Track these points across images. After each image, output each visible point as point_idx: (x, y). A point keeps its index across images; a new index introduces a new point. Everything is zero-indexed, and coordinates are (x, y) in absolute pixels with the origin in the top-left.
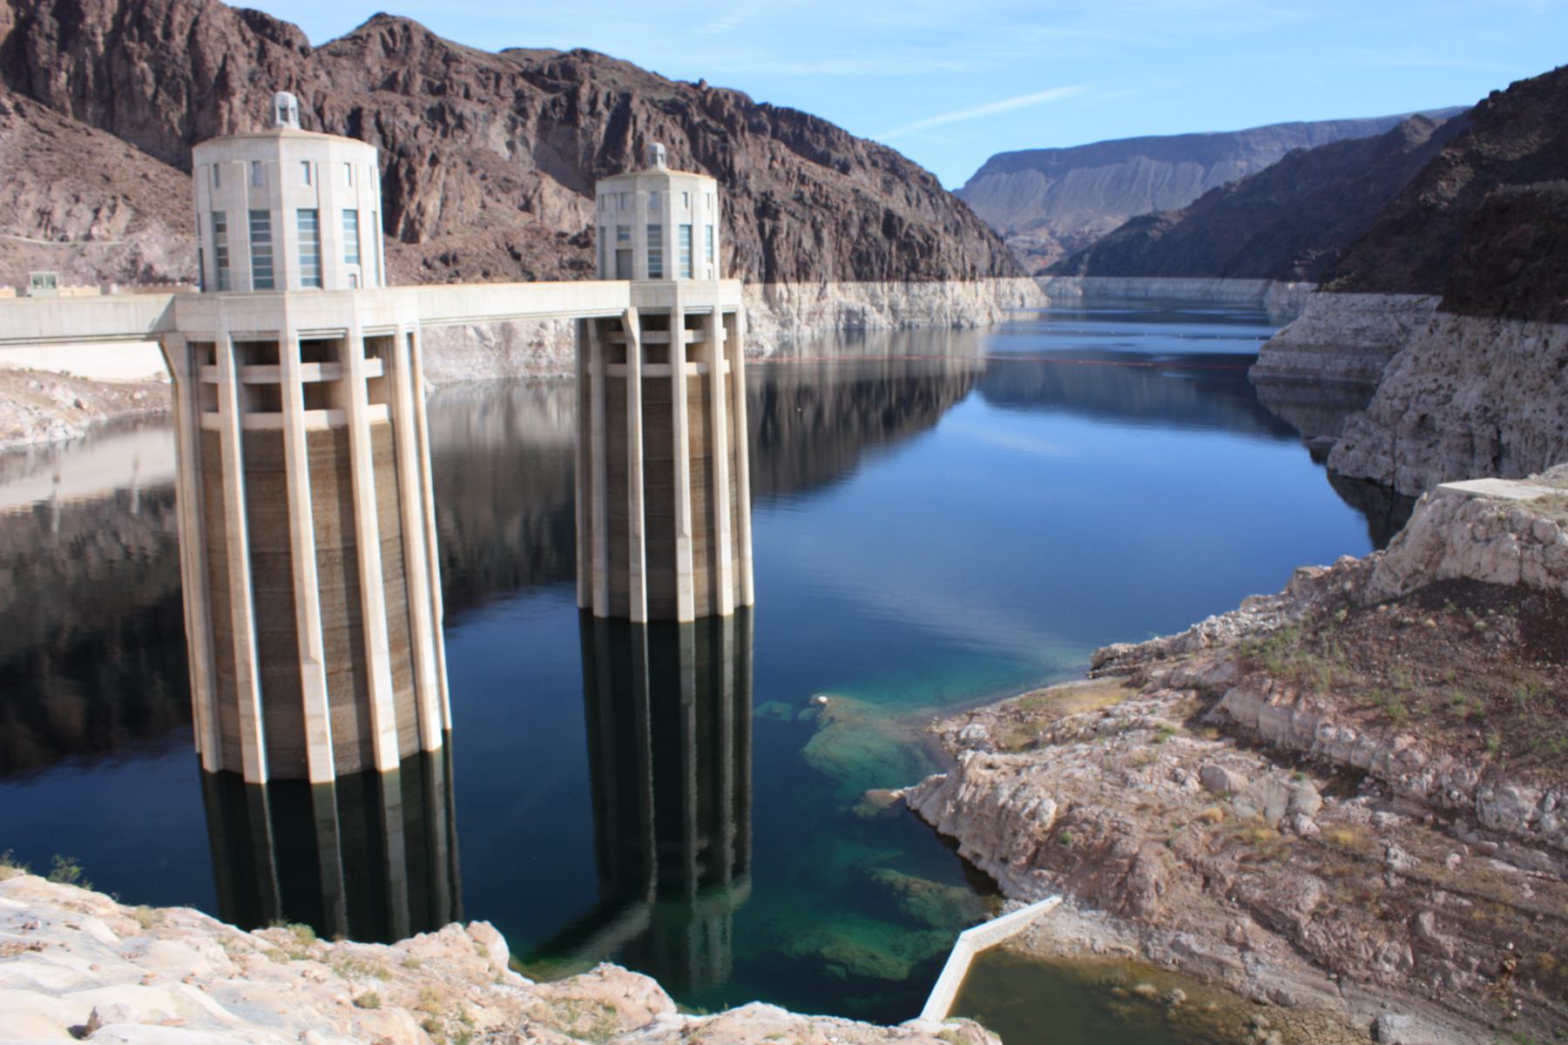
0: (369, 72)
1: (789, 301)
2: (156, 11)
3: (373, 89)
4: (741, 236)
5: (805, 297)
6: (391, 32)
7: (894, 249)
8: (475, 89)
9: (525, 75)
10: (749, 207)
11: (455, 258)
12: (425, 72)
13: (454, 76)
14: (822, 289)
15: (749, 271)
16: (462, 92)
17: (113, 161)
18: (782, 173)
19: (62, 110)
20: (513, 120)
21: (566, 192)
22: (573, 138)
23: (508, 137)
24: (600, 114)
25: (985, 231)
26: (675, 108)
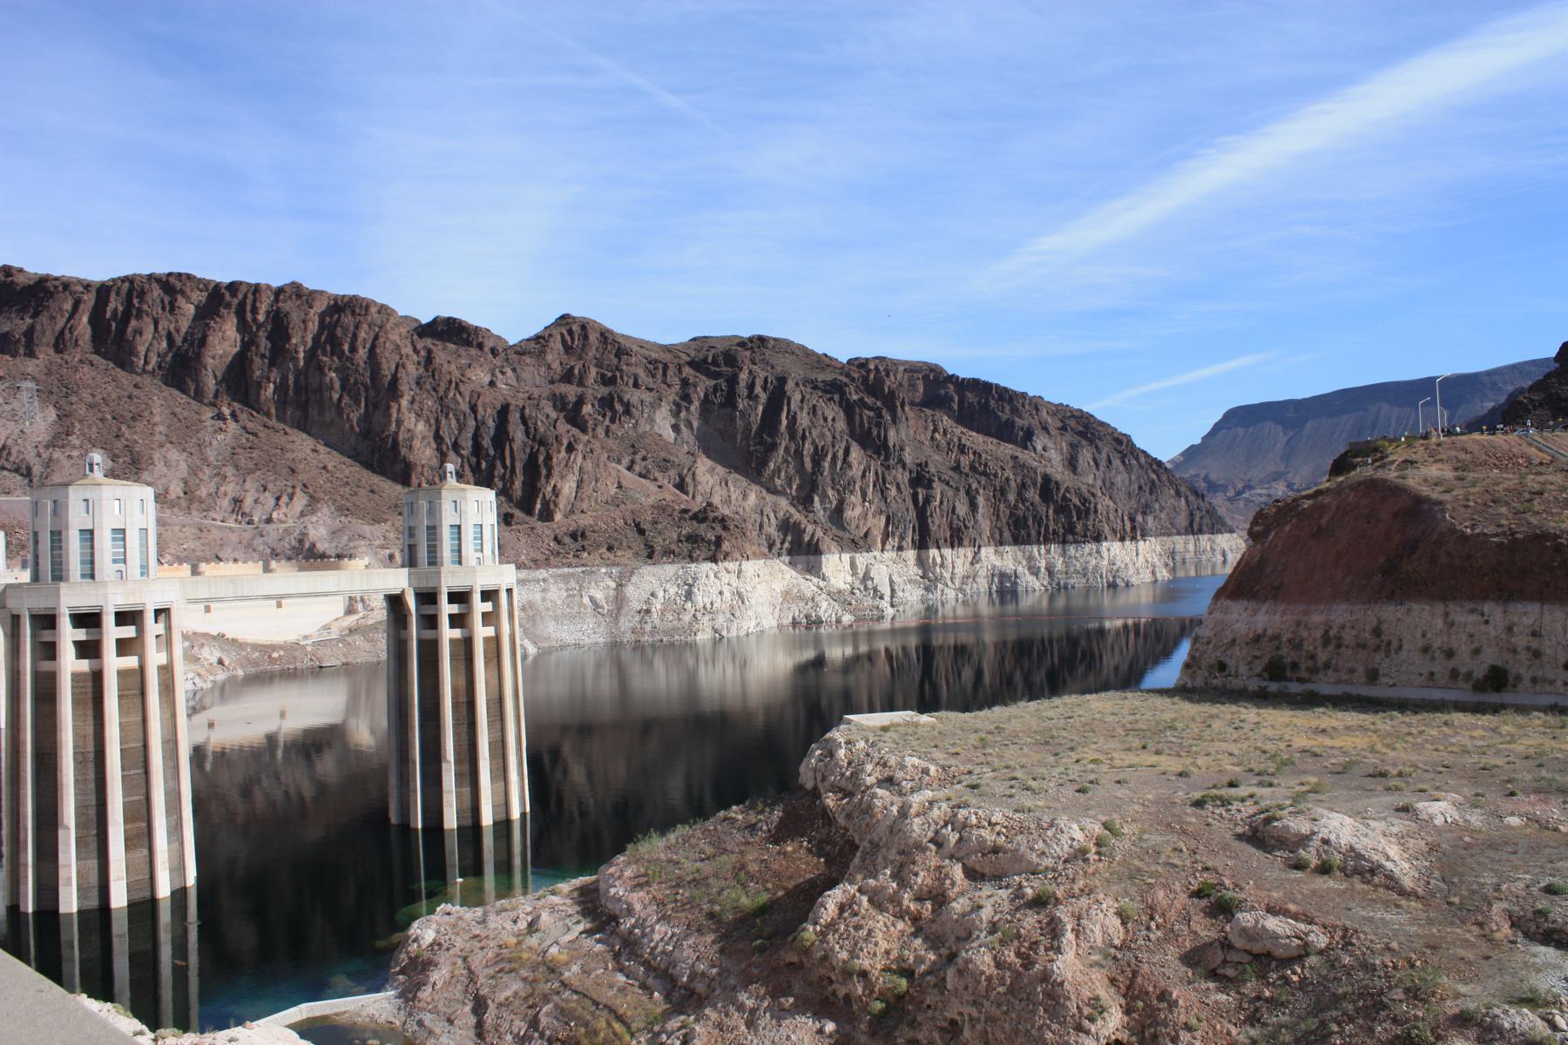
0: (549, 367)
1: (942, 565)
2: (345, 330)
3: (552, 382)
4: (894, 505)
5: (959, 562)
6: (570, 332)
7: (1051, 512)
9: (691, 364)
10: (903, 477)
11: (583, 535)
13: (625, 368)
15: (902, 538)
16: (631, 382)
17: (301, 455)
18: (943, 443)
19: (268, 415)
20: (678, 405)
21: (720, 470)
22: (733, 419)
23: (673, 421)
25: (1183, 489)
26: (833, 389)
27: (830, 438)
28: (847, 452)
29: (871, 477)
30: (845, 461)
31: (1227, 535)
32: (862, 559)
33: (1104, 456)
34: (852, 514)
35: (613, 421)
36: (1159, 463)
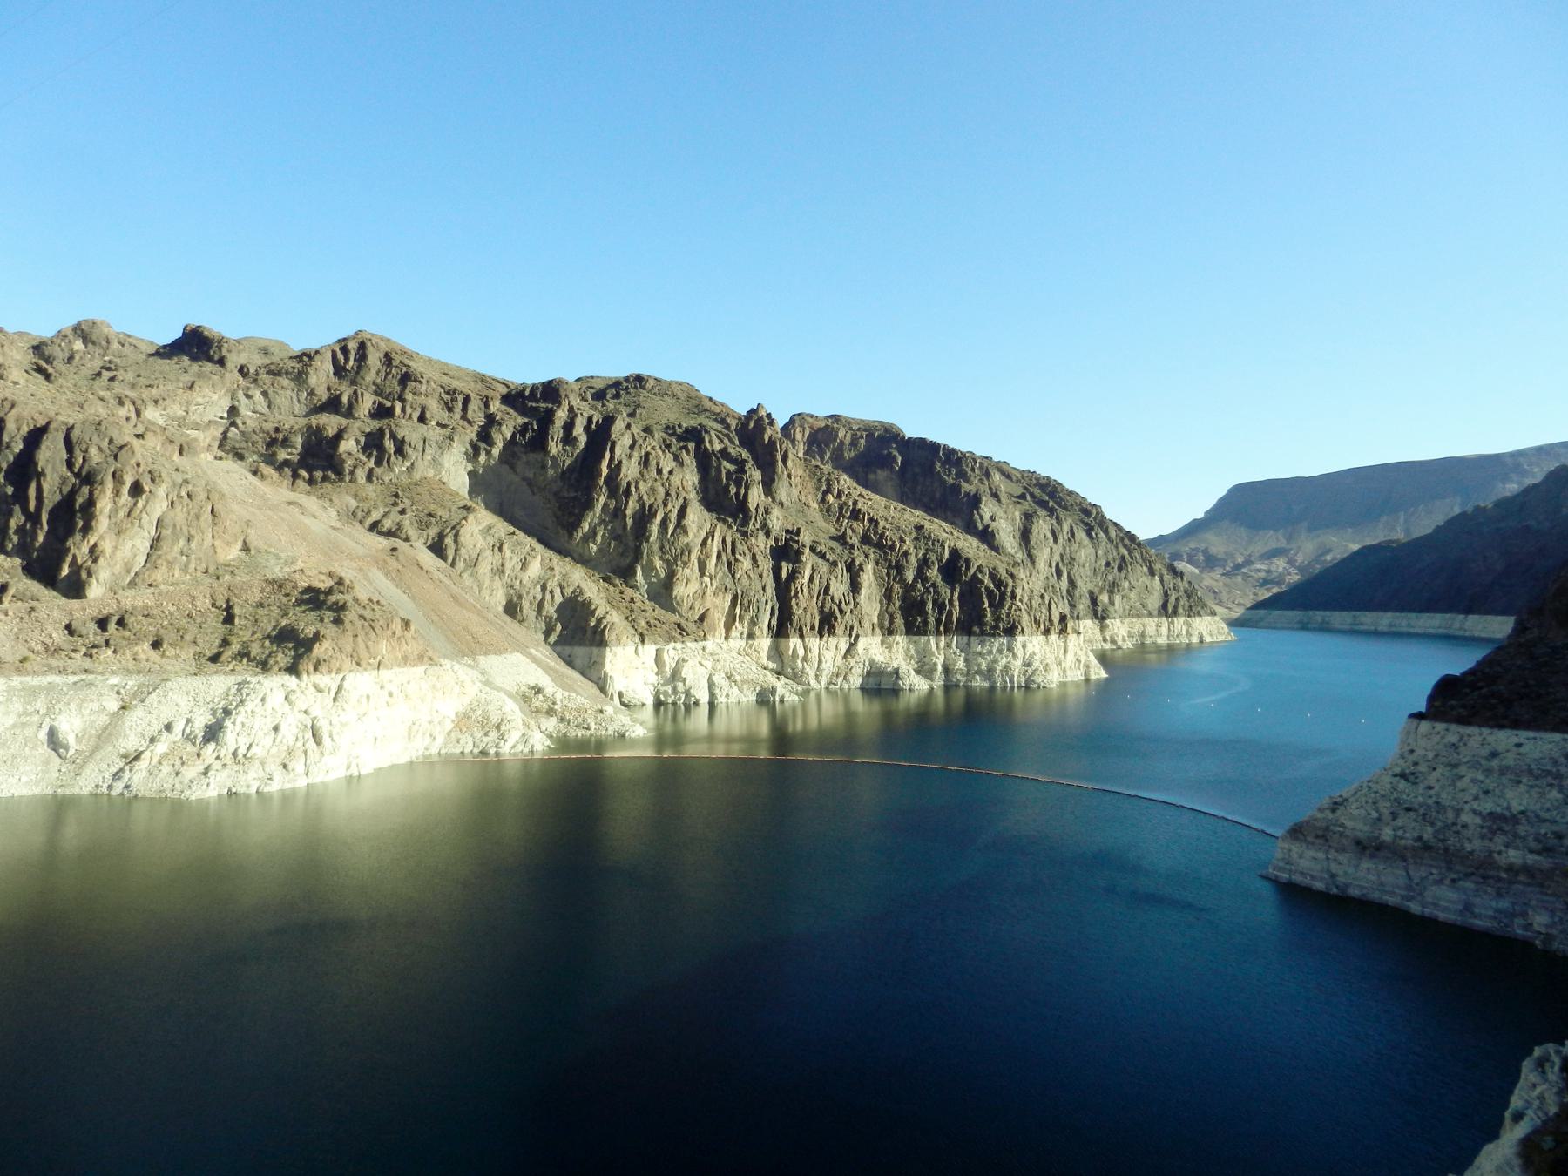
1: (805, 659)
4: (745, 581)
5: (828, 656)
8: (435, 410)
10: (762, 544)
12: (379, 392)
14: (852, 645)
16: (416, 415)
22: (544, 467)
23: (470, 467)
24: (575, 439)
25: (1157, 566)
27: (661, 491)
28: (682, 513)
29: (715, 546)
30: (679, 524)
31: (1207, 619)
32: (671, 653)
33: (1066, 527)
34: (685, 590)
35: (378, 463)
36: (1132, 538)
